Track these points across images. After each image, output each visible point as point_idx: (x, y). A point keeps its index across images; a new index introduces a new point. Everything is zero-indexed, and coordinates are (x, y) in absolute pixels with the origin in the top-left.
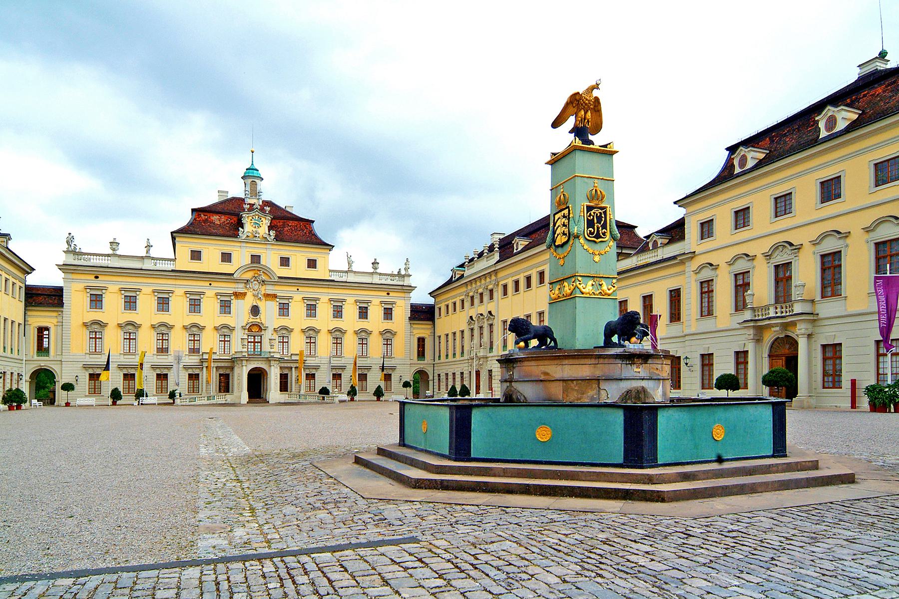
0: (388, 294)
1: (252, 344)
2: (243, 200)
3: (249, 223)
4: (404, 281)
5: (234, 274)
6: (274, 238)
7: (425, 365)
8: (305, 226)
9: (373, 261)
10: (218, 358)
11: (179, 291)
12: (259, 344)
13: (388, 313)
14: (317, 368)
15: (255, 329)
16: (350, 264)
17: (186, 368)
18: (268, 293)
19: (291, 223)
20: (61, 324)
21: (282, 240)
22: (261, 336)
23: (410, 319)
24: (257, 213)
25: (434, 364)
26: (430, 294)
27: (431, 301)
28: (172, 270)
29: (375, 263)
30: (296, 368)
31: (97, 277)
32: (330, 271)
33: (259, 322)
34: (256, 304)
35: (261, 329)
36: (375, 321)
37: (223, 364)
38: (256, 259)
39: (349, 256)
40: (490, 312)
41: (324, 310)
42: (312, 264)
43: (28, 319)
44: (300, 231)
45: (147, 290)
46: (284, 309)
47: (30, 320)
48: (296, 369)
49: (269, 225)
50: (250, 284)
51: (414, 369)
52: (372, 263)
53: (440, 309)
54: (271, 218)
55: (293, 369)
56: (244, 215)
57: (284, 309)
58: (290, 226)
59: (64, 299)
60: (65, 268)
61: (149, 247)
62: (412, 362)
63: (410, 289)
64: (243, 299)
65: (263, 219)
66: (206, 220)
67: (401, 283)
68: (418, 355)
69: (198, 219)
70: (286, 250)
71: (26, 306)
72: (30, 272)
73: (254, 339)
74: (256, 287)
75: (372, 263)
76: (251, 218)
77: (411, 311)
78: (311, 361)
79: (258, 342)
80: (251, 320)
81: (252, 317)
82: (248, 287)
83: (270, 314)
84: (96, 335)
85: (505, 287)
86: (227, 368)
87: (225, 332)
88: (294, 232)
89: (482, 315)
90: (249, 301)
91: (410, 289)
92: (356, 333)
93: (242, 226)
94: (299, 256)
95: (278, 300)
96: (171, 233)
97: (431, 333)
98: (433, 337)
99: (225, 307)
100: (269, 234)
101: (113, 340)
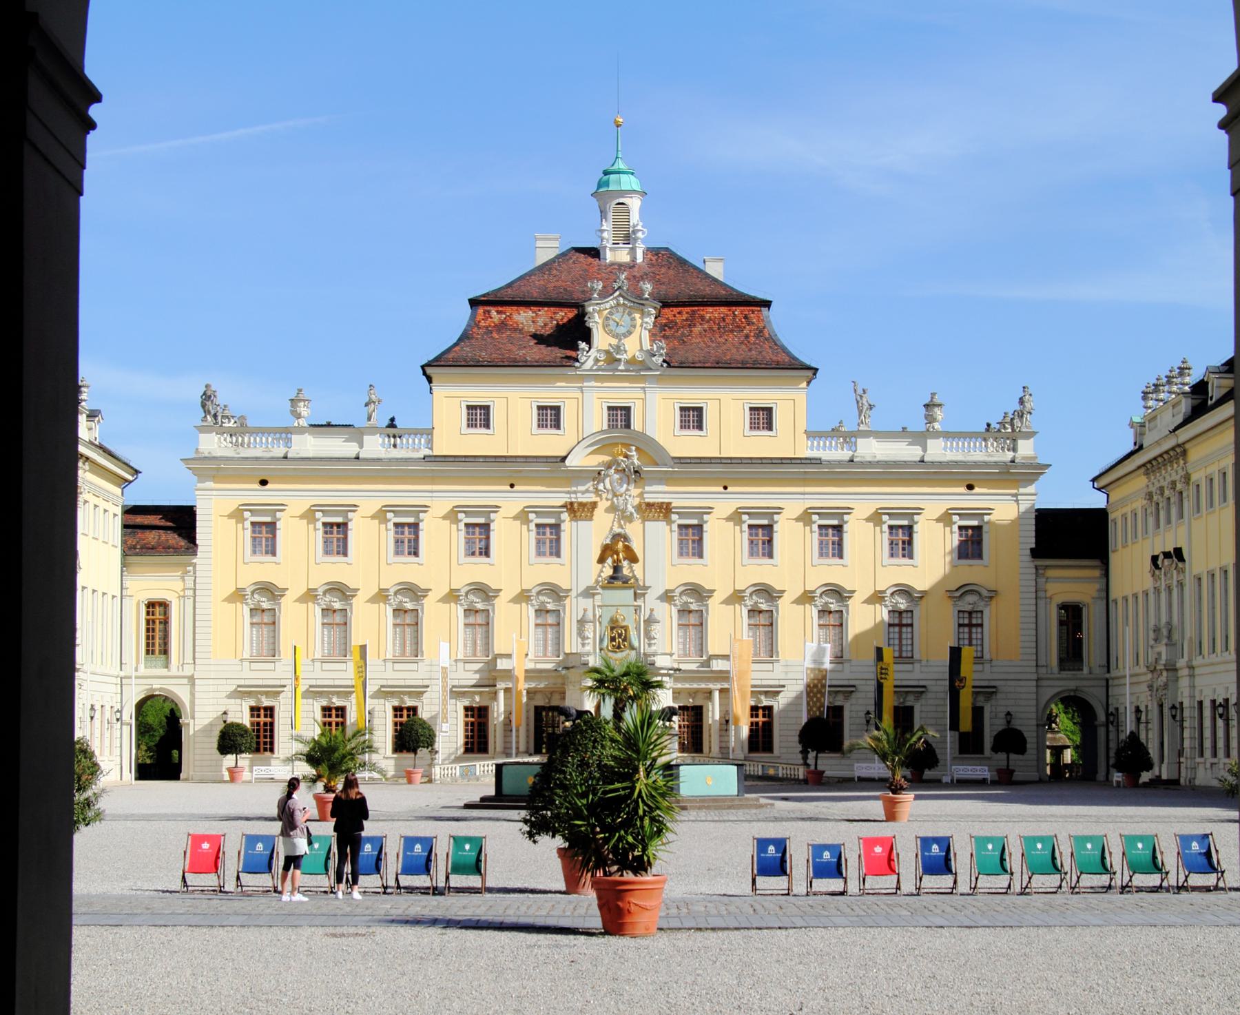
2: (594, 253)
3: (600, 327)
4: (1014, 450)
5: (564, 459)
6: (664, 361)
7: (1083, 681)
8: (746, 317)
9: (927, 401)
16: (863, 407)
18: (651, 501)
19: (710, 313)
23: (1035, 553)
26: (1093, 480)
27: (1097, 501)
29: (939, 405)
30: (721, 691)
31: (264, 483)
38: (621, 415)
44: (732, 331)
48: (723, 695)
52: (924, 406)
54: (655, 308)
55: (716, 695)
58: (708, 322)
59: (198, 536)
66: (502, 326)
69: (483, 324)
71: (125, 554)
72: (130, 478)
75: (924, 406)
77: (1037, 531)
82: (601, 487)
88: (717, 336)
89: (1167, 555)
93: (587, 336)
95: (674, 517)
96: (423, 367)
97: (1098, 591)
98: (1105, 601)
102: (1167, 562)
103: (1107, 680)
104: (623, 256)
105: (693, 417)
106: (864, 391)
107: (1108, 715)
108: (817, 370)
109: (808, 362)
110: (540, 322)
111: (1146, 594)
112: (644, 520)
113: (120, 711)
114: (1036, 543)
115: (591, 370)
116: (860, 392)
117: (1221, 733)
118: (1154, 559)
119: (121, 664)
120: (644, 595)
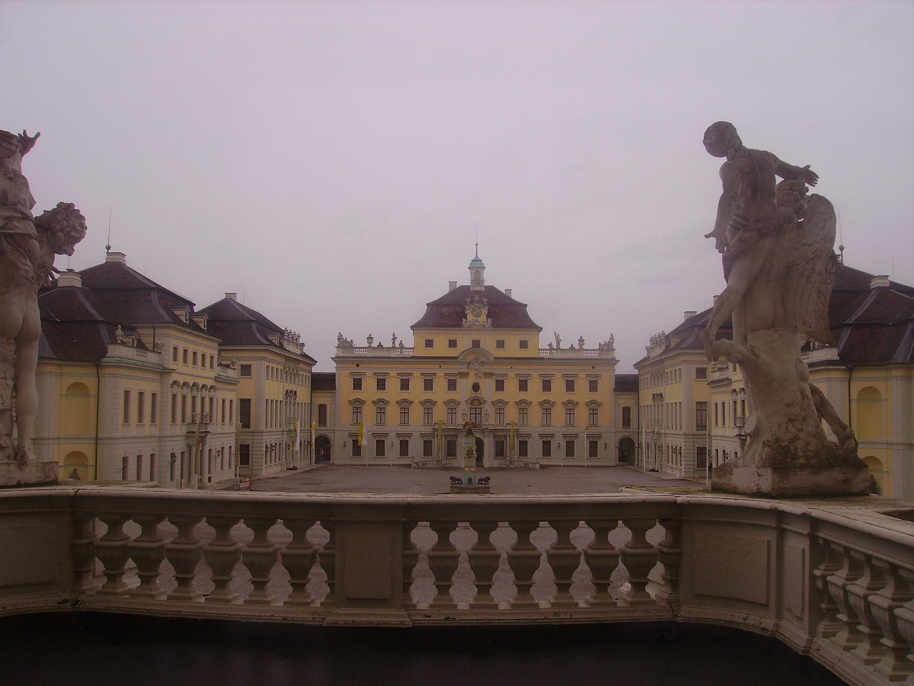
0: (593, 368)
1: (474, 415)
2: (468, 287)
9: (579, 338)
10: (447, 427)
11: (417, 374)
12: (480, 416)
13: (593, 386)
14: (529, 436)
15: (476, 403)
16: (558, 342)
17: (422, 435)
20: (334, 402)
21: (497, 327)
22: (481, 409)
24: (477, 304)
25: (638, 432)
26: (634, 365)
27: (636, 372)
28: (412, 357)
32: (539, 350)
33: (479, 397)
34: (476, 382)
35: (480, 404)
36: (582, 393)
37: (450, 433)
38: (476, 343)
39: (557, 335)
40: (661, 394)
41: (535, 385)
42: (524, 345)
43: (313, 399)
45: (393, 373)
46: (500, 386)
47: (314, 400)
49: (487, 313)
50: (472, 365)
51: (619, 436)
53: (641, 380)
56: (466, 308)
57: (500, 386)
60: (336, 359)
61: (394, 338)
62: (617, 430)
63: (614, 361)
64: (466, 378)
65: (482, 309)
67: (606, 357)
68: (623, 424)
70: (501, 335)
73: (476, 411)
74: (476, 367)
75: (579, 340)
76: (472, 309)
78: (523, 430)
79: (478, 414)
80: (473, 396)
81: (474, 393)
83: (488, 390)
84: (357, 410)
85: (667, 373)
86: (453, 436)
87: (452, 406)
89: (658, 395)
90: (471, 380)
91: (614, 361)
92: (564, 404)
94: (512, 340)
95: (494, 377)
96: (411, 327)
99: (452, 385)
100: (487, 321)
101: (369, 413)
102: (658, 397)
103: (638, 432)
104: (478, 288)
105: (500, 344)
106: (558, 335)
107: (639, 444)
108: (542, 328)
109: (539, 325)
110: (450, 311)
111: (651, 405)
112: (485, 378)
113: (310, 442)
114: (616, 386)
115: (467, 328)
116: (557, 335)
117: (674, 457)
118: (654, 395)
119: (311, 426)
120: (484, 403)
